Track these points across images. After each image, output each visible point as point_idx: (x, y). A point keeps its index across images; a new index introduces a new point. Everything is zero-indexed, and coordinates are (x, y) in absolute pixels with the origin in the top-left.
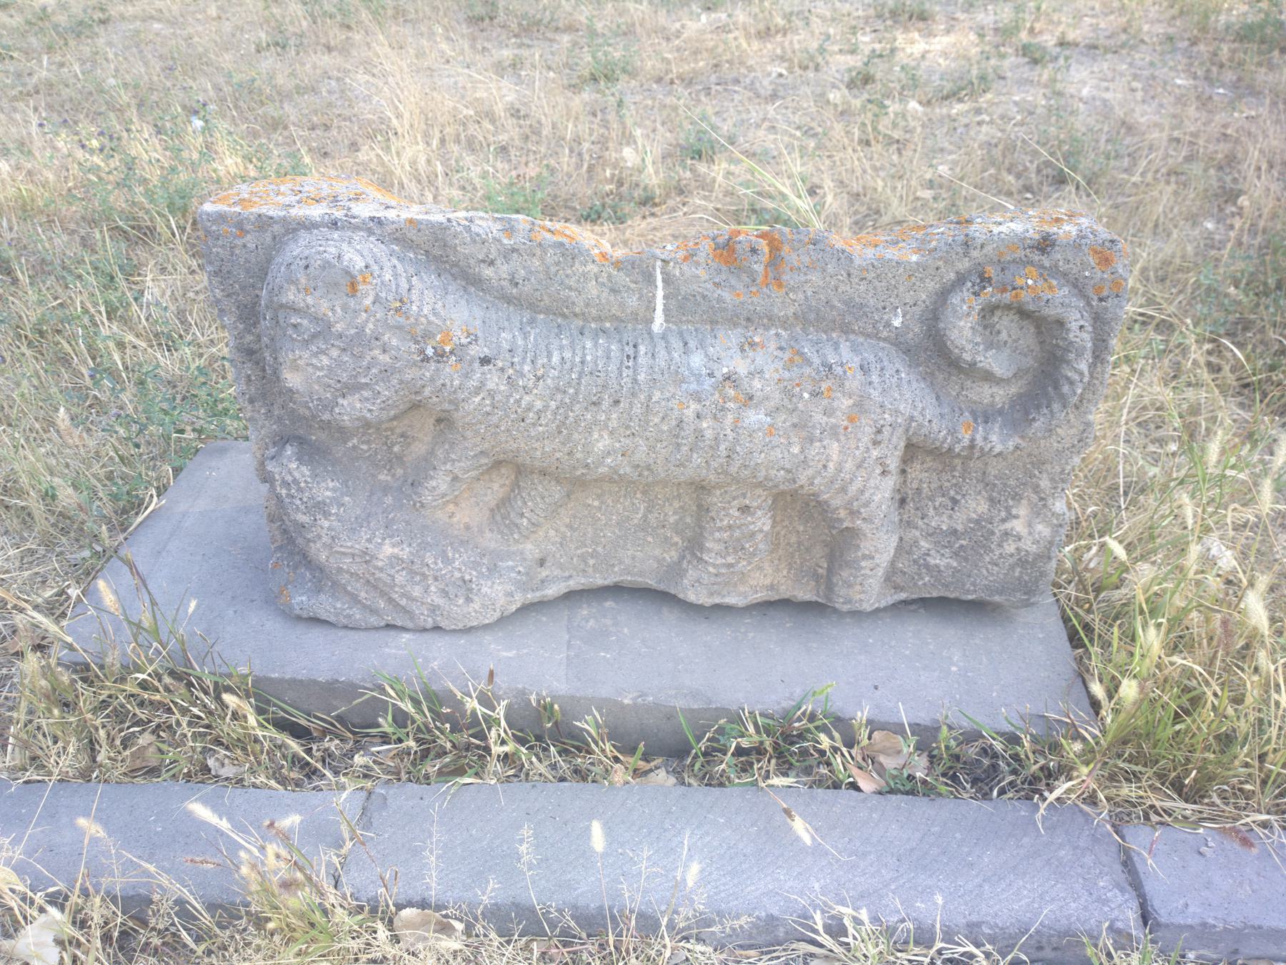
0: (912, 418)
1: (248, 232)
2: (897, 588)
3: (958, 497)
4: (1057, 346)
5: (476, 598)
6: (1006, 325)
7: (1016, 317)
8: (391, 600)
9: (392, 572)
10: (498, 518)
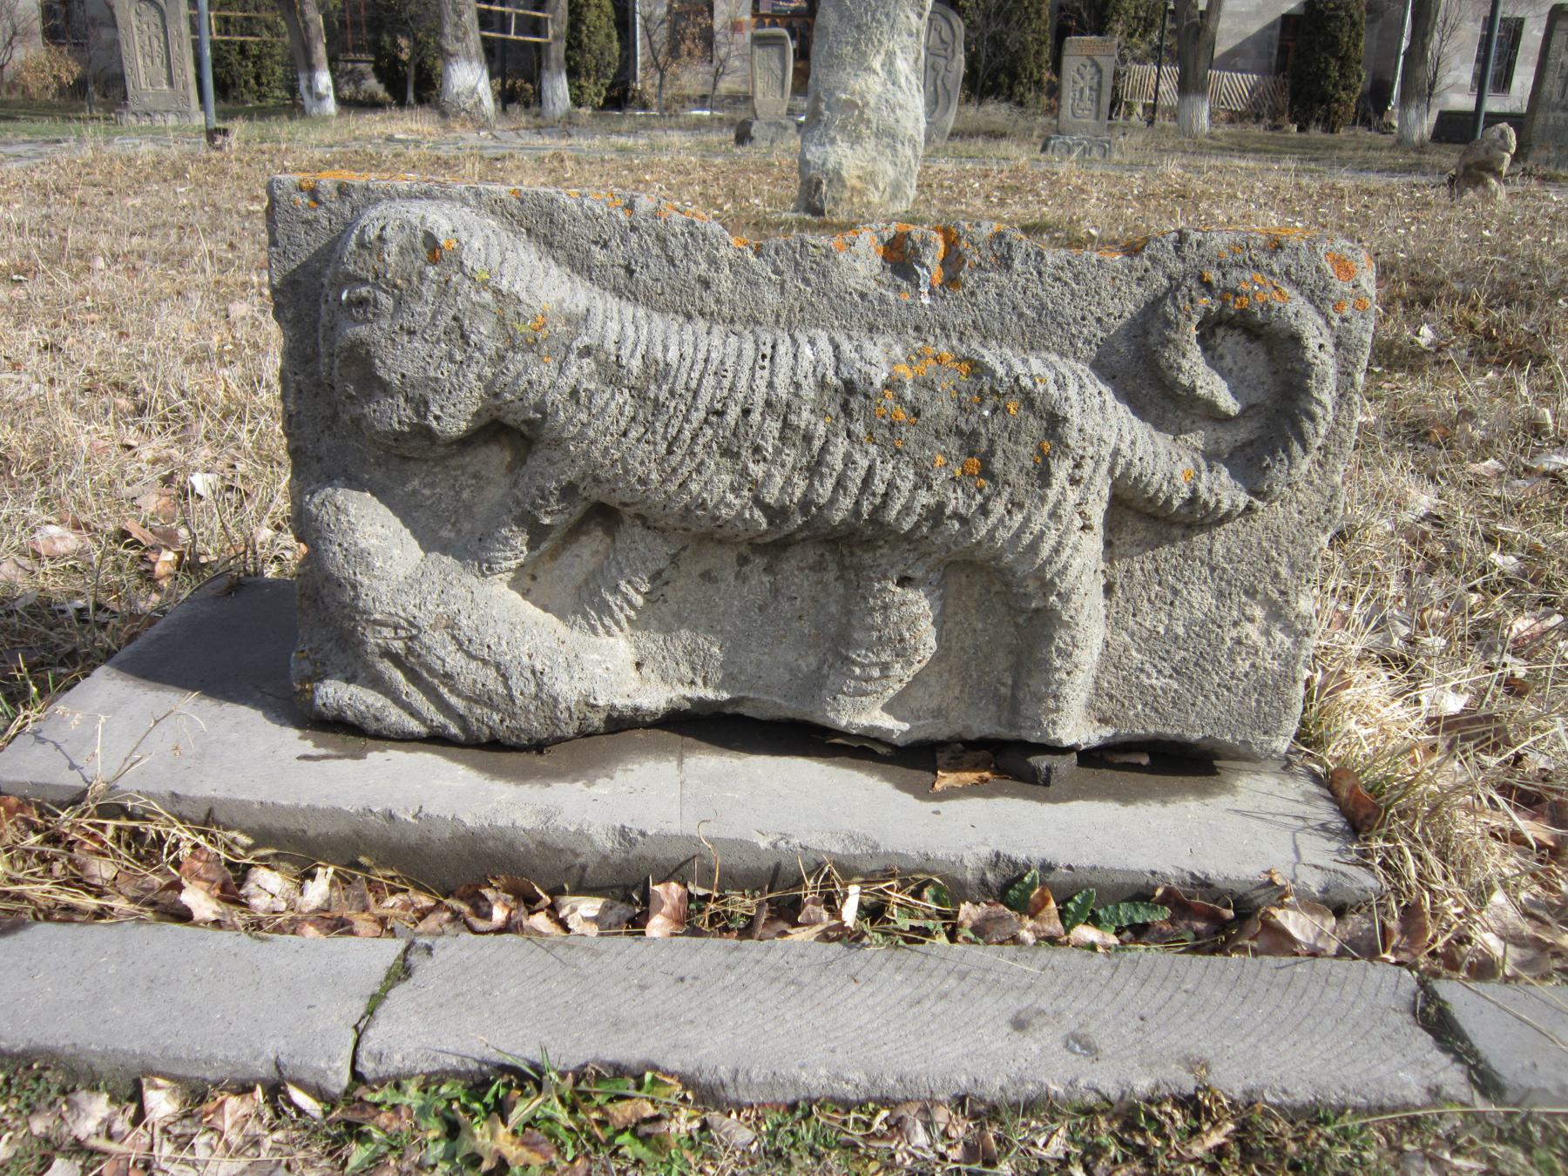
3: (1180, 586)
4: (1293, 370)
6: (1229, 343)
7: (1243, 338)
9: (442, 653)
10: (585, 595)
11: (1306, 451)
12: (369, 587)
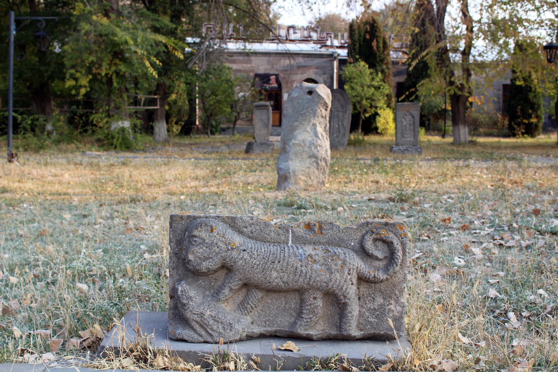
2: (361, 330)
6: (380, 244)
8: (207, 331)
11: (397, 266)
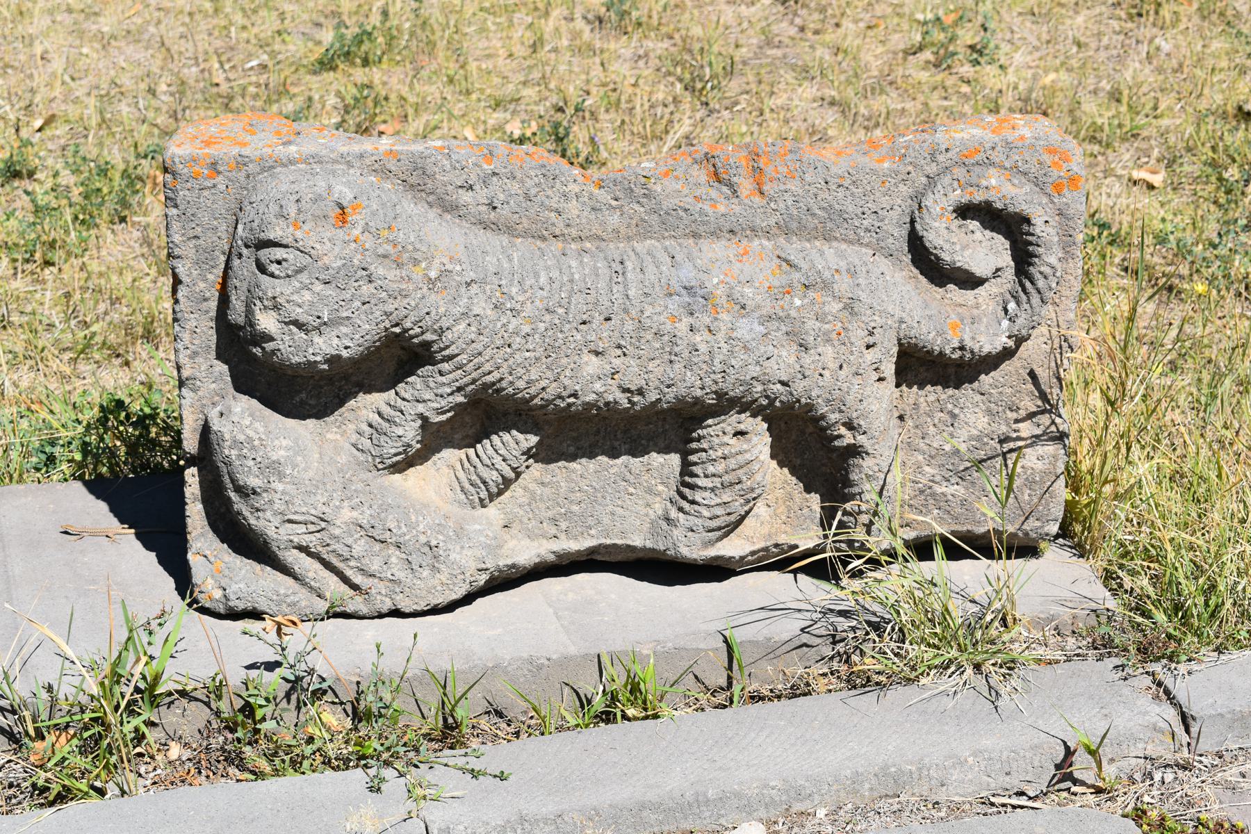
0: (901, 321)
1: (219, 173)
3: (956, 411)
5: (442, 567)
8: (345, 580)
9: (349, 541)
12: (283, 493)
